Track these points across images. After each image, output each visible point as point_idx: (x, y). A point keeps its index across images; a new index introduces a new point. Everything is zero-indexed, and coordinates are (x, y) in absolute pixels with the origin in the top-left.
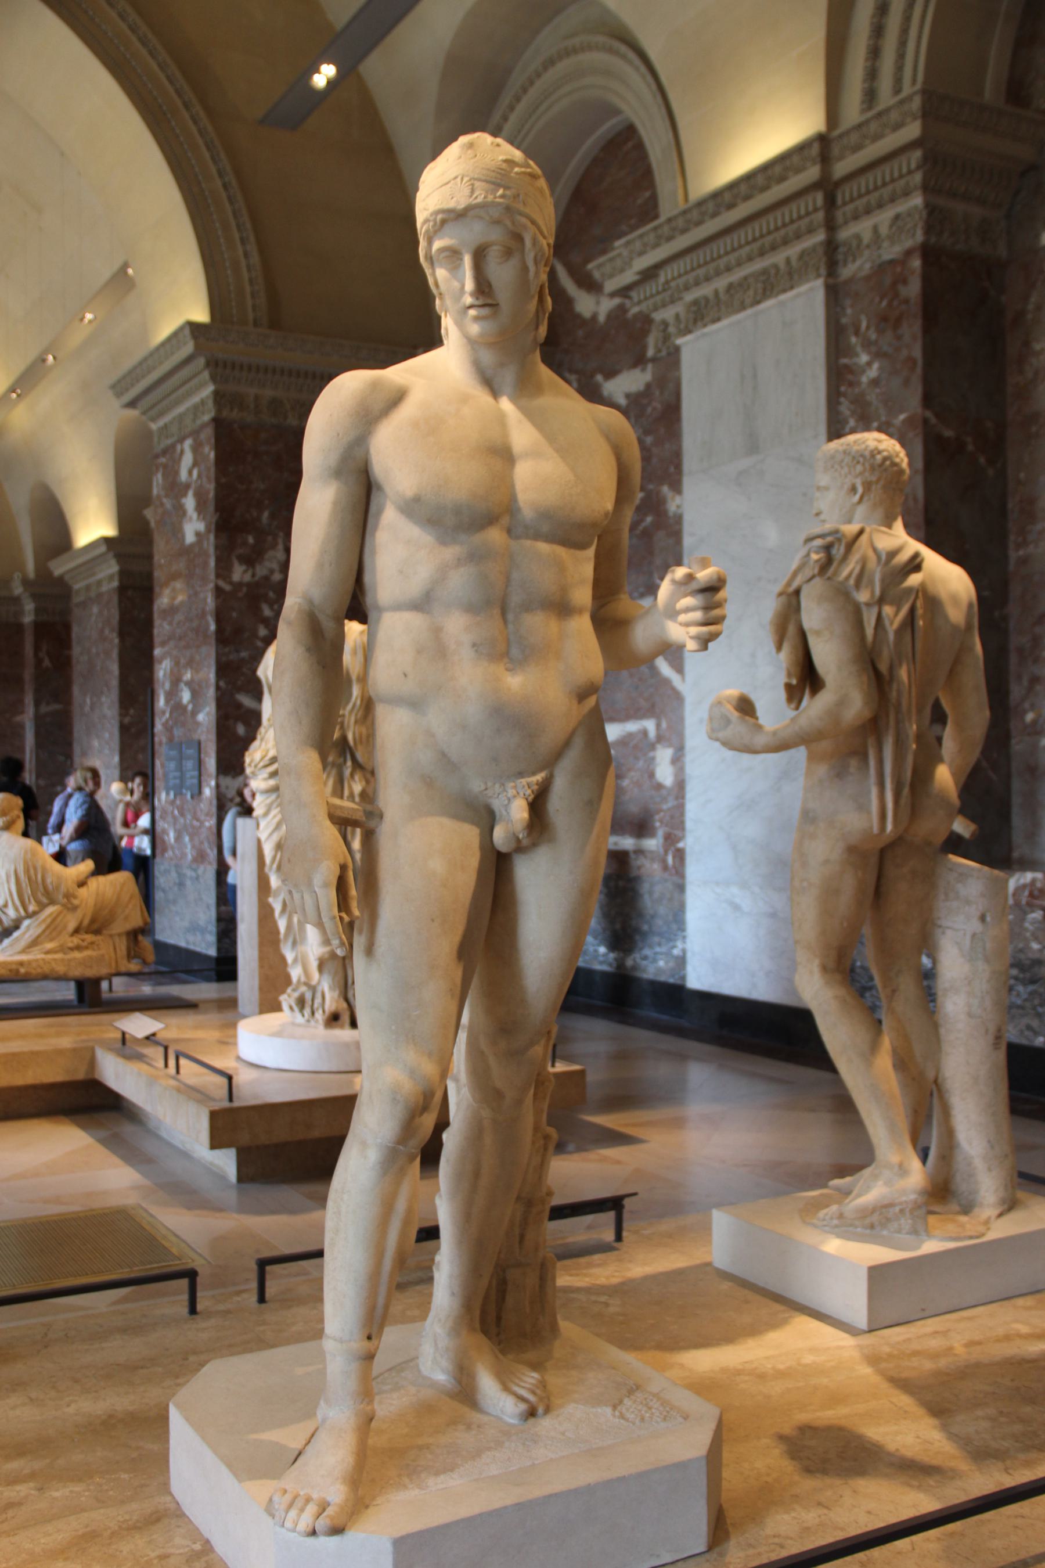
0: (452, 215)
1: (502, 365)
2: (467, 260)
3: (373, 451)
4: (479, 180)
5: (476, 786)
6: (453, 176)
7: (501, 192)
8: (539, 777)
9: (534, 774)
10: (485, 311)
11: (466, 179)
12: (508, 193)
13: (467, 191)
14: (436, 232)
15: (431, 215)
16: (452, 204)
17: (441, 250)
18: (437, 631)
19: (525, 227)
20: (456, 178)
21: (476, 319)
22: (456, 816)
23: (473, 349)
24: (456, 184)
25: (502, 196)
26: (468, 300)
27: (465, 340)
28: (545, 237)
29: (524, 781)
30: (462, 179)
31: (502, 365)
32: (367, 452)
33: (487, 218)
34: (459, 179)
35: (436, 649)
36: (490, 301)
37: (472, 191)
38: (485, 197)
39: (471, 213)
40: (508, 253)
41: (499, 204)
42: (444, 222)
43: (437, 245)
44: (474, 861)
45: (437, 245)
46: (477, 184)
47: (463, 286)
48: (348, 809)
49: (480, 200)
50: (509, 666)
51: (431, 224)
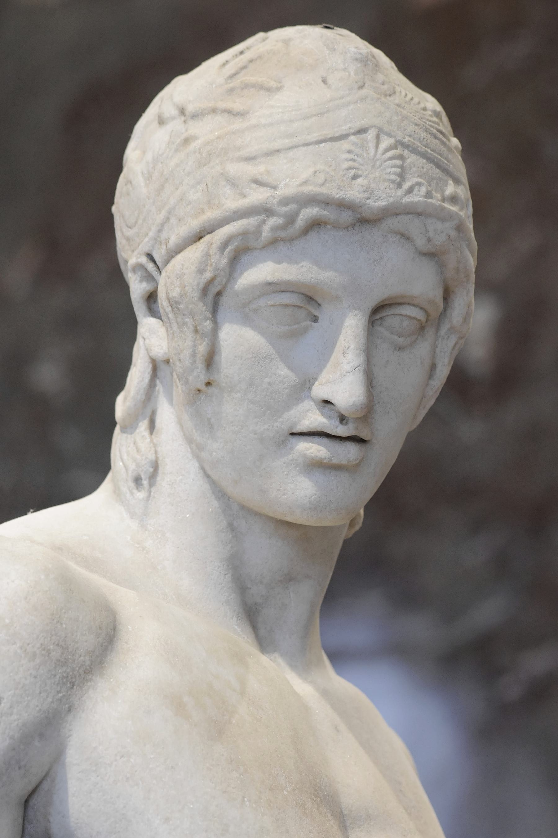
0: (346, 217)
1: (289, 579)
2: (351, 328)
3: (72, 756)
4: (414, 151)
6: (357, 125)
10: (351, 452)
11: (386, 142)
14: (274, 242)
15: (285, 201)
16: (353, 193)
17: (274, 287)
20: (362, 131)
21: (316, 466)
23: (231, 527)
24: (363, 147)
26: (314, 419)
27: (215, 503)
30: (378, 137)
31: (289, 579)
32: (58, 757)
33: (420, 242)
34: (371, 135)
37: (402, 176)
38: (428, 195)
39: (392, 223)
41: (451, 216)
42: (315, 225)
43: (260, 272)
45: (260, 272)
46: (411, 158)
47: (304, 385)
49: (417, 197)
51: (273, 221)
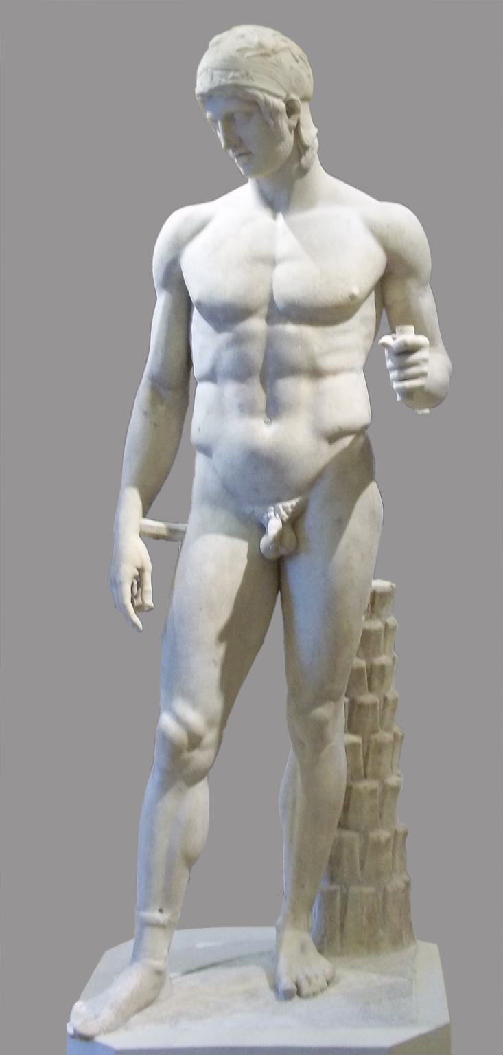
5: (248, 509)
7: (231, 74)
8: (294, 502)
9: (289, 499)
12: (237, 74)
13: (209, 79)
18: (220, 397)
19: (256, 97)
22: (230, 534)
25: (233, 78)
28: (278, 97)
29: (280, 506)
35: (219, 409)
36: (242, 151)
37: (212, 78)
40: (249, 115)
44: (242, 564)
46: (216, 73)
48: (157, 528)
50: (268, 420)
